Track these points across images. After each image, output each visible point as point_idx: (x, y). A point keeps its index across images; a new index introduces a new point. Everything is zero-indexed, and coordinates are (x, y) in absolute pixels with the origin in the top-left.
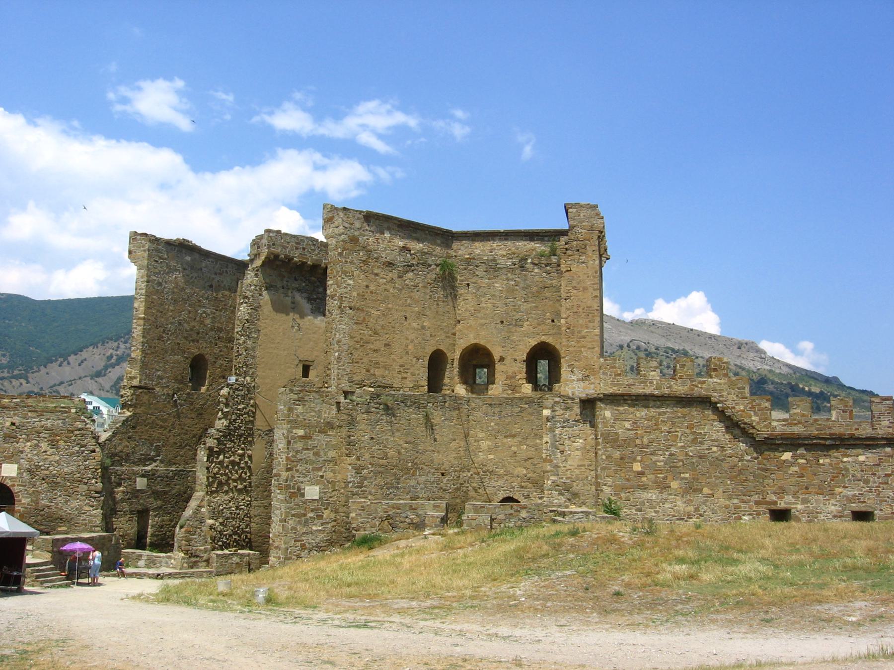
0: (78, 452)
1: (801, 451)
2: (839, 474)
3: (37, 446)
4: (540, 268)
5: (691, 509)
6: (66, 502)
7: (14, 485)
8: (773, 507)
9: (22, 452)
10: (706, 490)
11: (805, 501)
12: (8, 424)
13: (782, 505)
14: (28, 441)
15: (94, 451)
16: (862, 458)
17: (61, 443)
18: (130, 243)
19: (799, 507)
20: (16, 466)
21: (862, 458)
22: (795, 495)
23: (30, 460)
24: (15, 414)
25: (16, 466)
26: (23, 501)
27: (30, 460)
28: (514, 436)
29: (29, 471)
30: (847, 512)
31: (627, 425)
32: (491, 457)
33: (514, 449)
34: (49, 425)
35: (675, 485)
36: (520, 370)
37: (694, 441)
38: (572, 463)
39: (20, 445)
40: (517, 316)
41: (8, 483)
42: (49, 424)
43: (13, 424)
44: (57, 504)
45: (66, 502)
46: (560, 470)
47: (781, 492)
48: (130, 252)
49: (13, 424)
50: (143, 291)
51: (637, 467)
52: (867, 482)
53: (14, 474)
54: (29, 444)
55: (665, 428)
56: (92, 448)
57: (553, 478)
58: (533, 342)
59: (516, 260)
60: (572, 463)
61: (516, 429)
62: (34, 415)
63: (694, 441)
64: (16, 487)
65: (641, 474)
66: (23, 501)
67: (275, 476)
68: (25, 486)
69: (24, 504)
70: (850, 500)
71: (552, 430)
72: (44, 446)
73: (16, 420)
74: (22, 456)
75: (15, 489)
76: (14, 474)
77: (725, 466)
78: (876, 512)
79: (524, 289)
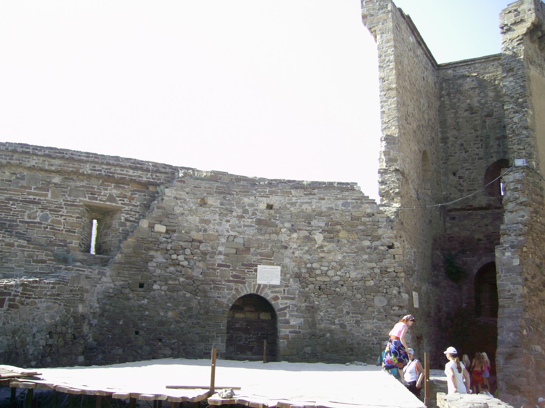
0: (369, 247)
3: (309, 239)
6: (358, 322)
7: (276, 298)
9: (286, 248)
12: (263, 206)
14: (293, 230)
15: (391, 247)
17: (343, 234)
18: (362, 7)
20: (279, 268)
23: (299, 261)
24: (272, 193)
25: (279, 268)
26: (292, 323)
29: (298, 276)
34: (324, 209)
39: (283, 237)
41: (269, 295)
42: (324, 206)
43: (270, 207)
44: (342, 326)
45: (358, 322)
48: (364, 17)
49: (270, 207)
53: (276, 281)
54: (295, 235)
56: (386, 241)
64: (280, 301)
66: (292, 323)
68: (293, 299)
69: (293, 326)
72: (319, 237)
73: (275, 200)
74: (288, 252)
75: (279, 304)
76: (276, 281)
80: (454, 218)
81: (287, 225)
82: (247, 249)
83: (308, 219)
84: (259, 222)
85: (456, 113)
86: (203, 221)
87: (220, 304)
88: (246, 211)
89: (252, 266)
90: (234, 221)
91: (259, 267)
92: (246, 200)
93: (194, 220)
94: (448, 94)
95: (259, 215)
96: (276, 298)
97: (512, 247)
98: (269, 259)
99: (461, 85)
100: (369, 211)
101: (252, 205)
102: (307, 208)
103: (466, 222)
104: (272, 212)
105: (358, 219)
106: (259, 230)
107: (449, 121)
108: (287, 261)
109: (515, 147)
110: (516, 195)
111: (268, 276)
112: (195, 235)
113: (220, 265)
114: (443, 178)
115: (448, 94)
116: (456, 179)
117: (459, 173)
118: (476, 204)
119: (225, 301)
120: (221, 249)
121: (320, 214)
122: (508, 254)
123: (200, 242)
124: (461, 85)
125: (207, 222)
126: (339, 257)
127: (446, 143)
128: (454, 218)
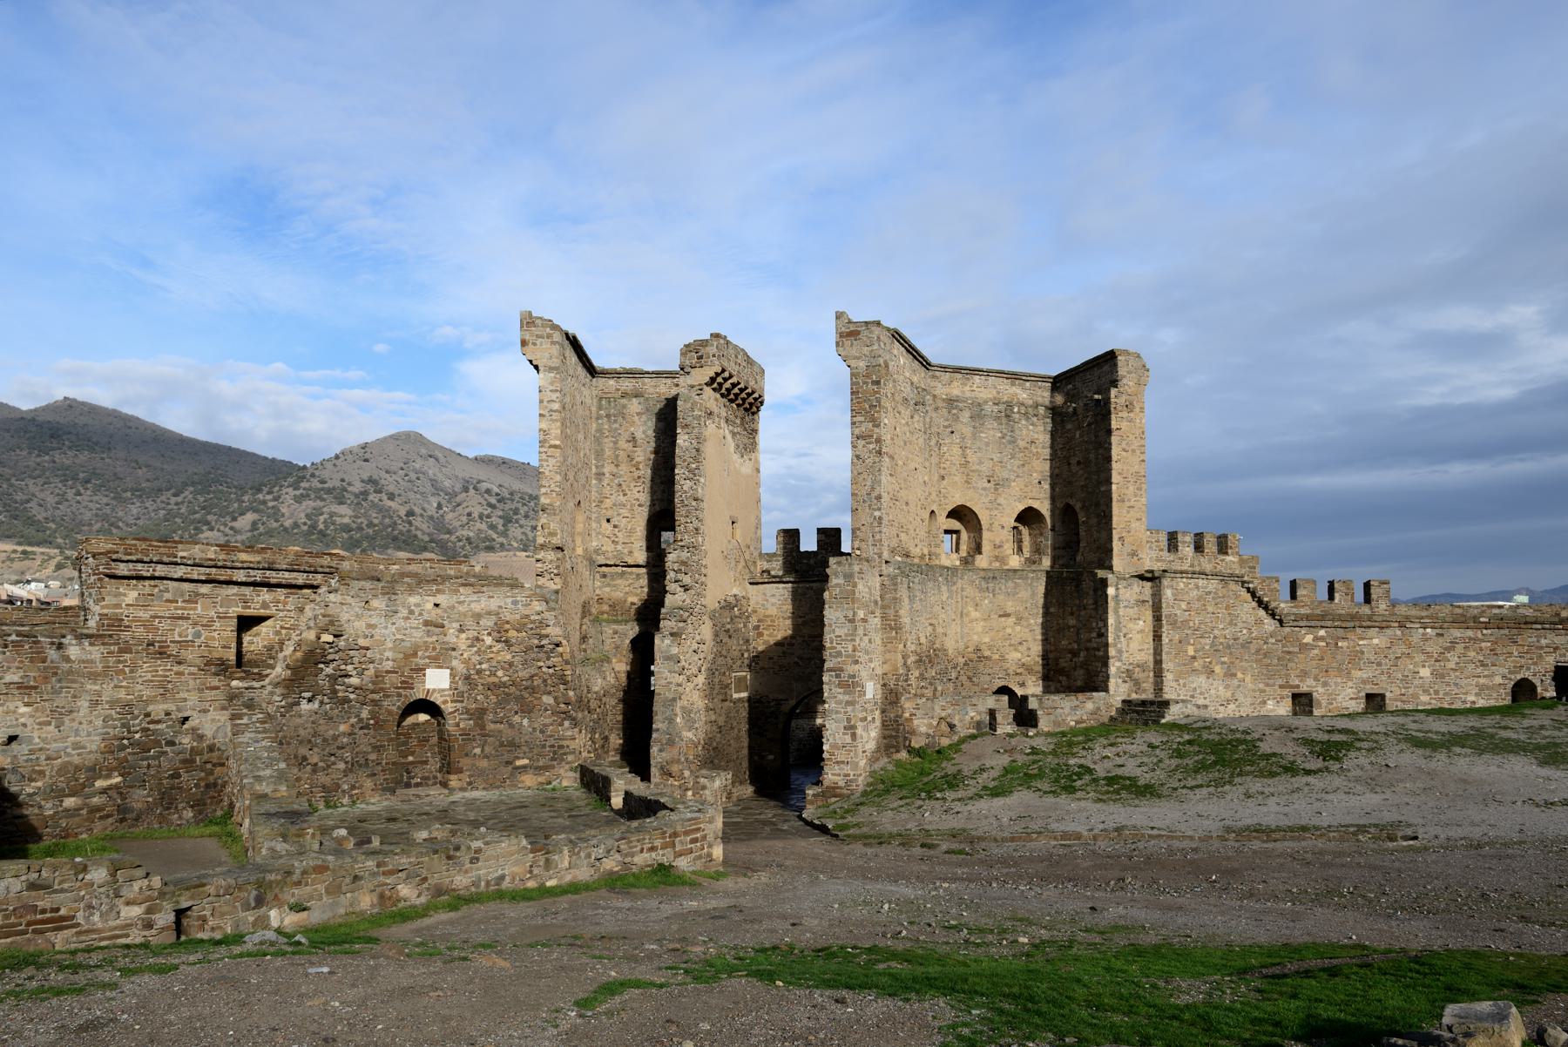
1: (1322, 633)
2: (1356, 656)
4: (1028, 419)
5: (1229, 694)
8: (1296, 691)
10: (1240, 675)
11: (1325, 684)
12: (430, 606)
13: (1304, 689)
14: (461, 630)
16: (1376, 641)
19: (1321, 690)
21: (1376, 641)
22: (1316, 679)
24: (438, 591)
27: (466, 662)
28: (1008, 615)
30: (1363, 694)
31: (1184, 606)
32: (987, 640)
33: (1009, 630)
35: (1218, 669)
36: (1006, 536)
37: (1231, 623)
38: (1134, 646)
40: (1005, 474)
41: (437, 699)
42: (494, 604)
46: (1125, 655)
47: (1304, 674)
49: (437, 605)
50: (556, 406)
51: (1191, 652)
52: (1379, 664)
54: (463, 636)
55: (1210, 609)
57: (1118, 664)
58: (1021, 507)
59: (1002, 407)
60: (1134, 646)
61: (1010, 606)
62: (469, 590)
63: (1231, 623)
65: (1194, 658)
67: (830, 670)
70: (1364, 682)
71: (1116, 612)
72: (489, 640)
77: (1253, 647)
78: (1388, 695)
79: (1010, 442)
80: (604, 576)
81: (456, 625)
82: (415, 654)
83: (477, 617)
84: (426, 623)
85: (615, 443)
86: (370, 626)
87: (390, 713)
88: (411, 612)
89: (420, 670)
90: (400, 623)
91: (428, 671)
92: (413, 600)
93: (360, 625)
94: (608, 416)
95: (426, 617)
96: (445, 702)
97: (672, 634)
98: (438, 661)
99: (624, 407)
100: (539, 608)
101: (417, 605)
102: (476, 608)
103: (619, 582)
104: (438, 611)
105: (527, 616)
106: (428, 633)
107: (608, 453)
108: (455, 663)
109: (683, 520)
110: (680, 576)
111: (436, 681)
112: (362, 642)
113: (388, 672)
114: (594, 525)
115: (608, 416)
116: (609, 527)
117: (614, 521)
118: (631, 562)
119: (394, 708)
120: (389, 654)
121: (489, 613)
122: (667, 642)
123: (368, 649)
124: (624, 407)
125: (372, 626)
126: (509, 657)
127: (600, 480)
128: (604, 576)
